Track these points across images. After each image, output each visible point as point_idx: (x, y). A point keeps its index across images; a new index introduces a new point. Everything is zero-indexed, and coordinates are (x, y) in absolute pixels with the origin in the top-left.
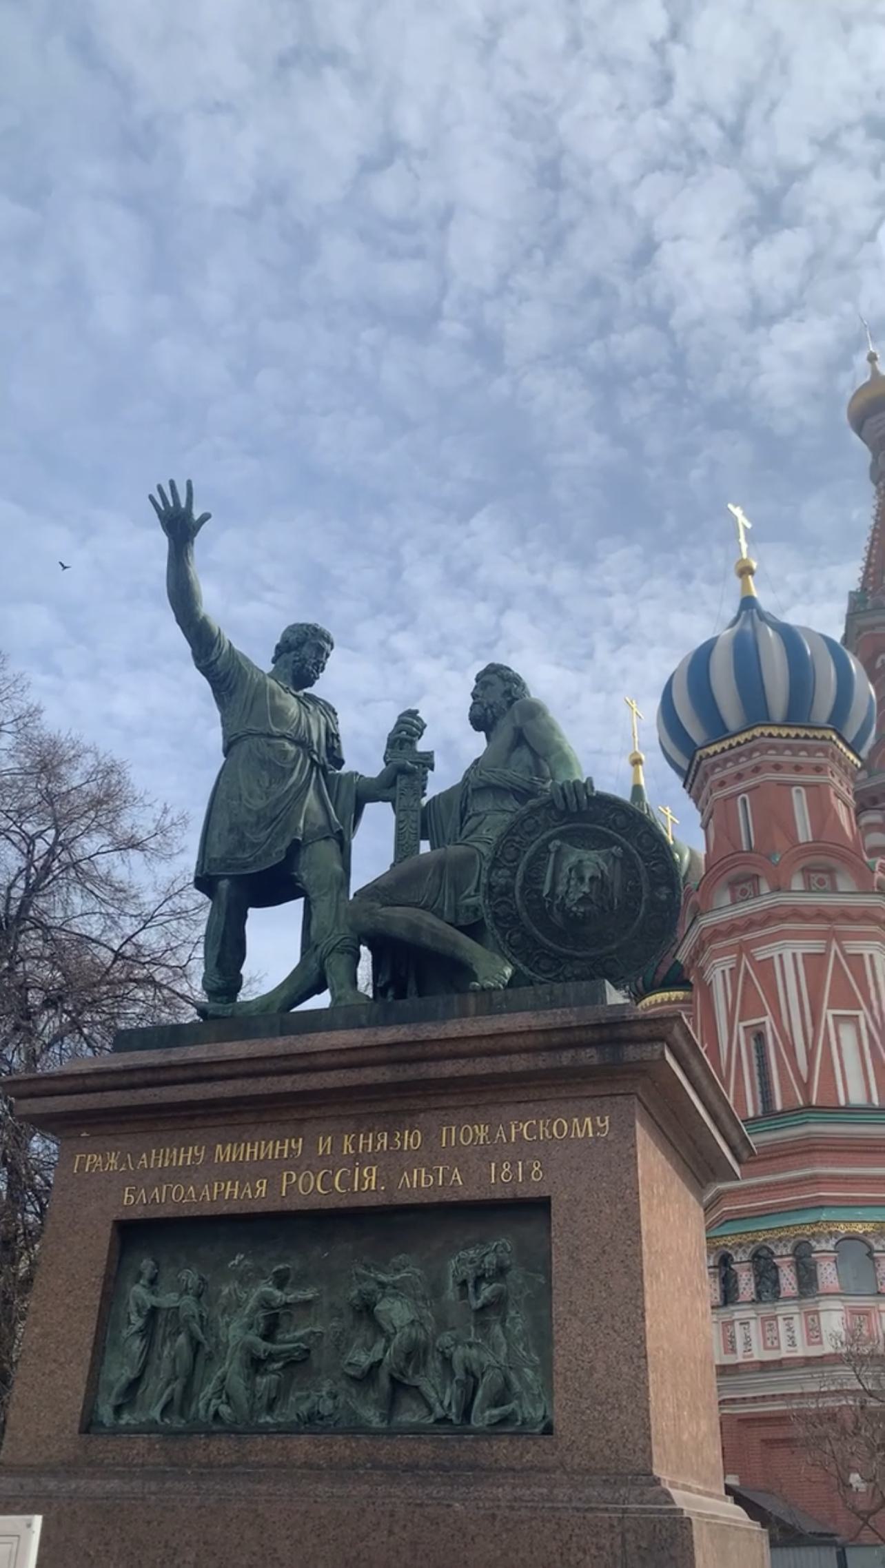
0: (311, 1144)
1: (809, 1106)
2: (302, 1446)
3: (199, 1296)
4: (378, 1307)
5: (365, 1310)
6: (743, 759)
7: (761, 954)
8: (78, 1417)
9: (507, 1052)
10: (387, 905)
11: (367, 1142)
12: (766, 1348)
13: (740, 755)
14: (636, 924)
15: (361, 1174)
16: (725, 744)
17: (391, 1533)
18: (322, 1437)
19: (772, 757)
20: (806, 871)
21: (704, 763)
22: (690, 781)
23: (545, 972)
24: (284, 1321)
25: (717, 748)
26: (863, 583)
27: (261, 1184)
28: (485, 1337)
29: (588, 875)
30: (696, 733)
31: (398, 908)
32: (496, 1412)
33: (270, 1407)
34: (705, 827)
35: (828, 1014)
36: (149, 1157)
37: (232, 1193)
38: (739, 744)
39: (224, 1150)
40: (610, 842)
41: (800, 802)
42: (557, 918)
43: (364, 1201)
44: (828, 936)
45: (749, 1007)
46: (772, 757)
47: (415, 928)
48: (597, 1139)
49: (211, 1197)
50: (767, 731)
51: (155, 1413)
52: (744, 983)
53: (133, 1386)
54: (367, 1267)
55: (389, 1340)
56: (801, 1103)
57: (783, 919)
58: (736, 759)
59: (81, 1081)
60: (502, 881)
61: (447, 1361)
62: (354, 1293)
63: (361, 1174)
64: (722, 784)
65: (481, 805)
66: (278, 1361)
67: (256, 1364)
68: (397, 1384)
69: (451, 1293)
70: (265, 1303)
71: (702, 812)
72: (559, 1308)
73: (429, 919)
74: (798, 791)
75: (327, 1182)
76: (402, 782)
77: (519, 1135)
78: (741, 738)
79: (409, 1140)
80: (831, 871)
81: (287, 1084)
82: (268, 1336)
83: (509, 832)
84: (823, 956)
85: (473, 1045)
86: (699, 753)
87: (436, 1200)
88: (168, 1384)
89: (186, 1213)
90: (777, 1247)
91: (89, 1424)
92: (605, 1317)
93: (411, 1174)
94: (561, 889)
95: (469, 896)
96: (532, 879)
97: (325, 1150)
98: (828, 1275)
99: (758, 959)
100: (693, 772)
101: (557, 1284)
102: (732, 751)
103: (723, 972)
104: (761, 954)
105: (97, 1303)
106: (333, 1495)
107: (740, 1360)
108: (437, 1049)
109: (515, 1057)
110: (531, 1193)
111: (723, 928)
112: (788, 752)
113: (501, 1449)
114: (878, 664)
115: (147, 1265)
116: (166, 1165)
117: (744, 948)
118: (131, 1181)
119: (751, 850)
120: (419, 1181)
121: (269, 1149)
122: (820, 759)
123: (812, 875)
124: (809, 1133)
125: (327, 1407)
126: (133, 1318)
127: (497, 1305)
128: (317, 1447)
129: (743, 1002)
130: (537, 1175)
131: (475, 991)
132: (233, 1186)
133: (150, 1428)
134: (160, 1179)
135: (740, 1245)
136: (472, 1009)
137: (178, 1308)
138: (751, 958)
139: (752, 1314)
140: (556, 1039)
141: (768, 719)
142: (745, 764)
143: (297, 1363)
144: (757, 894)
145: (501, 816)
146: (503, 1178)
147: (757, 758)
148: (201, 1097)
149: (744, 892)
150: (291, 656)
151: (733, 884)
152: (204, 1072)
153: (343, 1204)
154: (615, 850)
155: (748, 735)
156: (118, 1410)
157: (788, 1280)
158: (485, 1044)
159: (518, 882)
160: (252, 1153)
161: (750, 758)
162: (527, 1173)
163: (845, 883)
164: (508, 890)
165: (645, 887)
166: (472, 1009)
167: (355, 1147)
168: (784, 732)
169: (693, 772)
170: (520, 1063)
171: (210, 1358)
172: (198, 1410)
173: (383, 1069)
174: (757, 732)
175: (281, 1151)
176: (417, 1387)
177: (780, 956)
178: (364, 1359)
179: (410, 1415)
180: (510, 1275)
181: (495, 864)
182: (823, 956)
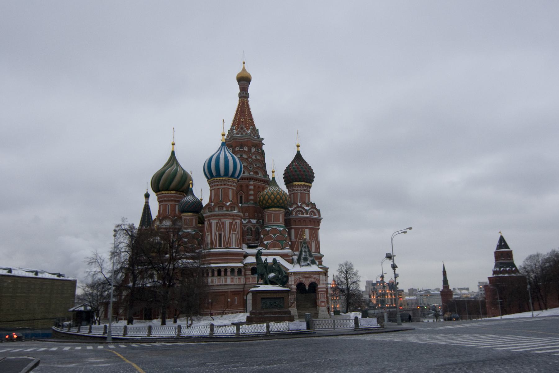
7: (223, 220)
30: (214, 173)
34: (211, 190)
44: (233, 219)
45: (220, 230)
46: (228, 183)
58: (221, 181)
64: (218, 185)
98: (229, 273)
104: (223, 220)
114: (236, 150)
117: (220, 219)
122: (235, 184)
142: (222, 183)
147: (225, 183)
151: (219, 207)
157: (223, 273)
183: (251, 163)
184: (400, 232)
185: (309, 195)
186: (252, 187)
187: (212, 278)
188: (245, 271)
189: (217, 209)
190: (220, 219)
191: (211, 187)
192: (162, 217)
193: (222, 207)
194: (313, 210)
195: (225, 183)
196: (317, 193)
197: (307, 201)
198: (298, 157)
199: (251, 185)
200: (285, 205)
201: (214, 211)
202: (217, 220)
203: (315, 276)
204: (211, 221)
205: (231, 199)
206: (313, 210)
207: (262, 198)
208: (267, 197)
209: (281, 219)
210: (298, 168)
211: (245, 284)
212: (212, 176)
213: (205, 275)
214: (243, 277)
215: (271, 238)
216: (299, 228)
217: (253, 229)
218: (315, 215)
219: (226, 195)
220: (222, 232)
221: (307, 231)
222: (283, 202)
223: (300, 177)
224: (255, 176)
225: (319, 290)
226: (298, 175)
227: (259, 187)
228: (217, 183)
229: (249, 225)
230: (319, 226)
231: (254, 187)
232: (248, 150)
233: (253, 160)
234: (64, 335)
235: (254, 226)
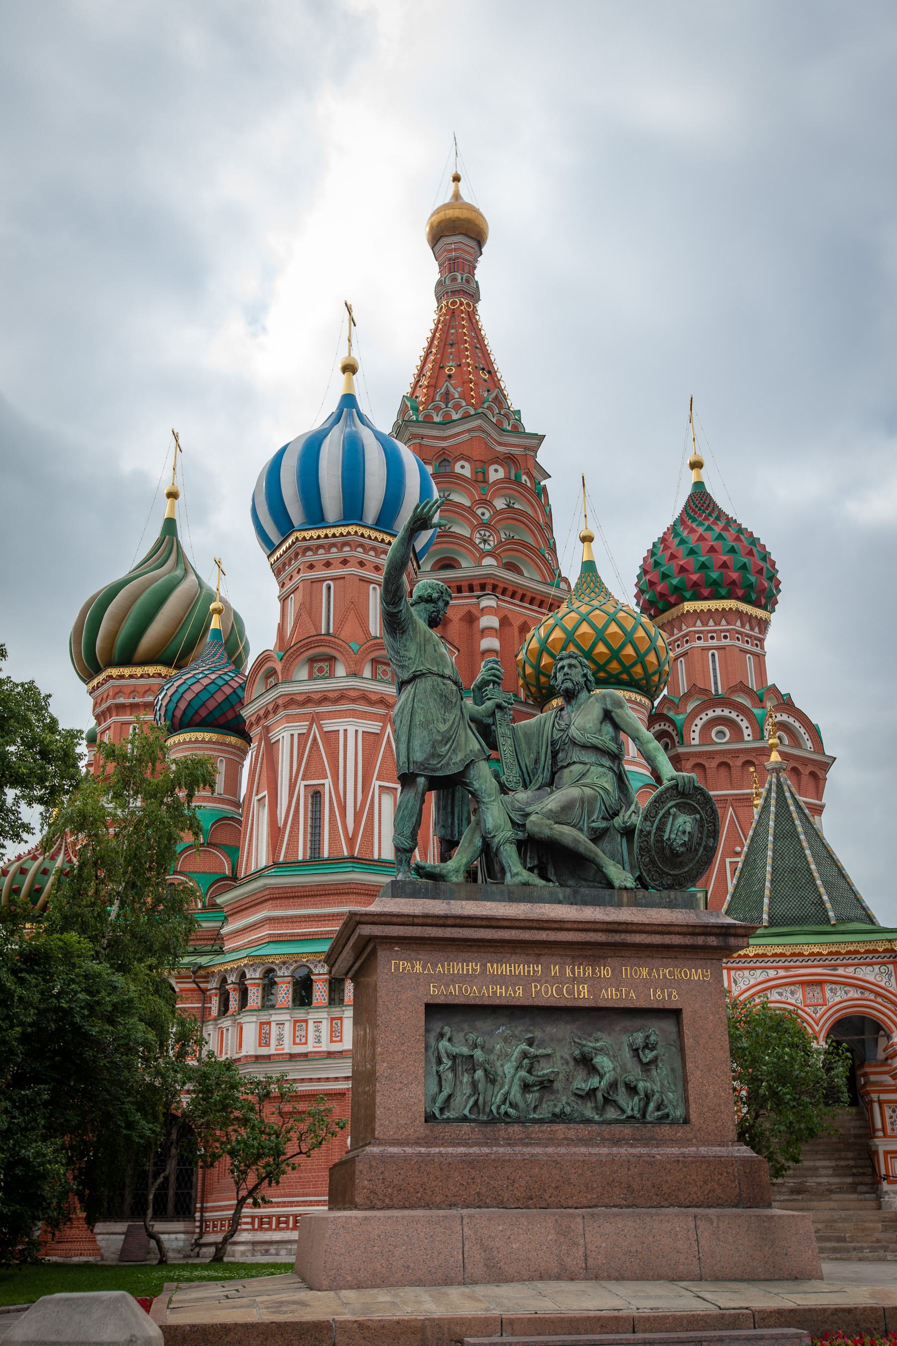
0: (547, 969)
1: (353, 857)
2: (560, 1129)
3: (483, 1048)
4: (595, 1060)
5: (585, 1062)
6: (334, 550)
7: (329, 725)
8: (423, 1115)
9: (669, 933)
10: (556, 823)
11: (579, 971)
12: (295, 1043)
13: (333, 545)
14: (697, 858)
15: (578, 988)
16: (322, 533)
17: (629, 1169)
18: (572, 1125)
19: (359, 553)
20: (375, 662)
21: (299, 544)
22: (278, 554)
23: (655, 881)
24: (536, 1065)
25: (314, 534)
26: (414, 389)
27: (519, 989)
28: (648, 1076)
29: (688, 829)
31: (565, 826)
32: (660, 1113)
33: (534, 1111)
34: (284, 599)
35: (376, 784)
36: (443, 966)
37: (501, 993)
38: (334, 536)
39: (492, 967)
40: (694, 811)
42: (668, 852)
43: (581, 1004)
45: (312, 768)
47: (575, 840)
48: (704, 981)
49: (489, 993)
50: (360, 530)
51: (466, 1112)
52: (311, 748)
53: (450, 1097)
54: (580, 1039)
55: (602, 1077)
56: (346, 854)
57: (354, 700)
59: (411, 919)
60: (648, 829)
61: (632, 1090)
62: (577, 1052)
63: (578, 988)
64: (311, 567)
65: (589, 757)
66: (536, 1086)
67: (526, 1087)
68: (607, 1100)
69: (627, 1054)
70: (525, 1055)
71: (283, 585)
72: (689, 1065)
73: (581, 835)
74: (374, 589)
75: (559, 991)
76: (498, 715)
77: (664, 975)
78: (337, 531)
79: (605, 972)
81: (543, 936)
82: (529, 1072)
83: (655, 801)
84: (378, 736)
85: (654, 928)
86: (298, 534)
87: (622, 1006)
88: (469, 1097)
89: (473, 1002)
90: (316, 966)
91: (430, 1118)
92: (713, 1069)
93: (607, 991)
94: (673, 836)
95: (593, 821)
96: (661, 829)
97: (556, 973)
99: (325, 729)
100: (284, 548)
101: (687, 1052)
102: (326, 541)
103: (292, 735)
105: (423, 1050)
106: (590, 1154)
107: (273, 1052)
108: (634, 928)
109: (672, 937)
110: (673, 1006)
111: (299, 698)
112: (372, 553)
113: (665, 1130)
115: (447, 1029)
116: (456, 972)
117: (315, 719)
118: (433, 980)
119: (328, 634)
120: (612, 995)
121: (521, 969)
123: (380, 666)
124: (352, 879)
125: (568, 1110)
126: (445, 1060)
127: (654, 1061)
128: (569, 1129)
129: (307, 764)
130: (675, 997)
131: (620, 889)
132: (501, 988)
133: (465, 1119)
134: (453, 980)
135: (284, 963)
136: (625, 900)
137: (472, 1056)
138: (320, 728)
139: (287, 1017)
140: (697, 930)
141: (361, 520)
143: (546, 1085)
144: (331, 675)
145: (600, 769)
146: (657, 997)
148: (490, 937)
149: (321, 670)
150: (430, 607)
151: (312, 660)
152: (494, 923)
153: (569, 1004)
154: (698, 816)
155: (344, 530)
156: (442, 1110)
158: (660, 928)
159: (654, 831)
160: (511, 971)
161: (340, 550)
162: (670, 995)
164: (649, 833)
165: (705, 839)
166: (625, 900)
167: (573, 971)
168: (374, 534)
169: (284, 548)
170: (676, 940)
171: (493, 1082)
172: (491, 1110)
173: (600, 934)
174: (352, 529)
175: (529, 972)
176: (614, 1101)
177: (346, 731)
178: (586, 1087)
179: (612, 1114)
180: (659, 1046)
181: (646, 818)
182: (378, 736)
183: (486, 526)
185: (760, 658)
187: (264, 1017)
193: (332, 659)
194: (784, 718)
197: (752, 683)
198: (700, 503)
200: (647, 676)
201: (287, 681)
202: (301, 727)
204: (274, 736)
206: (784, 718)
207: (534, 644)
210: (701, 538)
212: (285, 526)
213: (233, 1004)
222: (640, 659)
223: (714, 575)
226: (703, 566)
230: (819, 795)
231: (505, 621)
232: (475, 472)
233: (497, 513)
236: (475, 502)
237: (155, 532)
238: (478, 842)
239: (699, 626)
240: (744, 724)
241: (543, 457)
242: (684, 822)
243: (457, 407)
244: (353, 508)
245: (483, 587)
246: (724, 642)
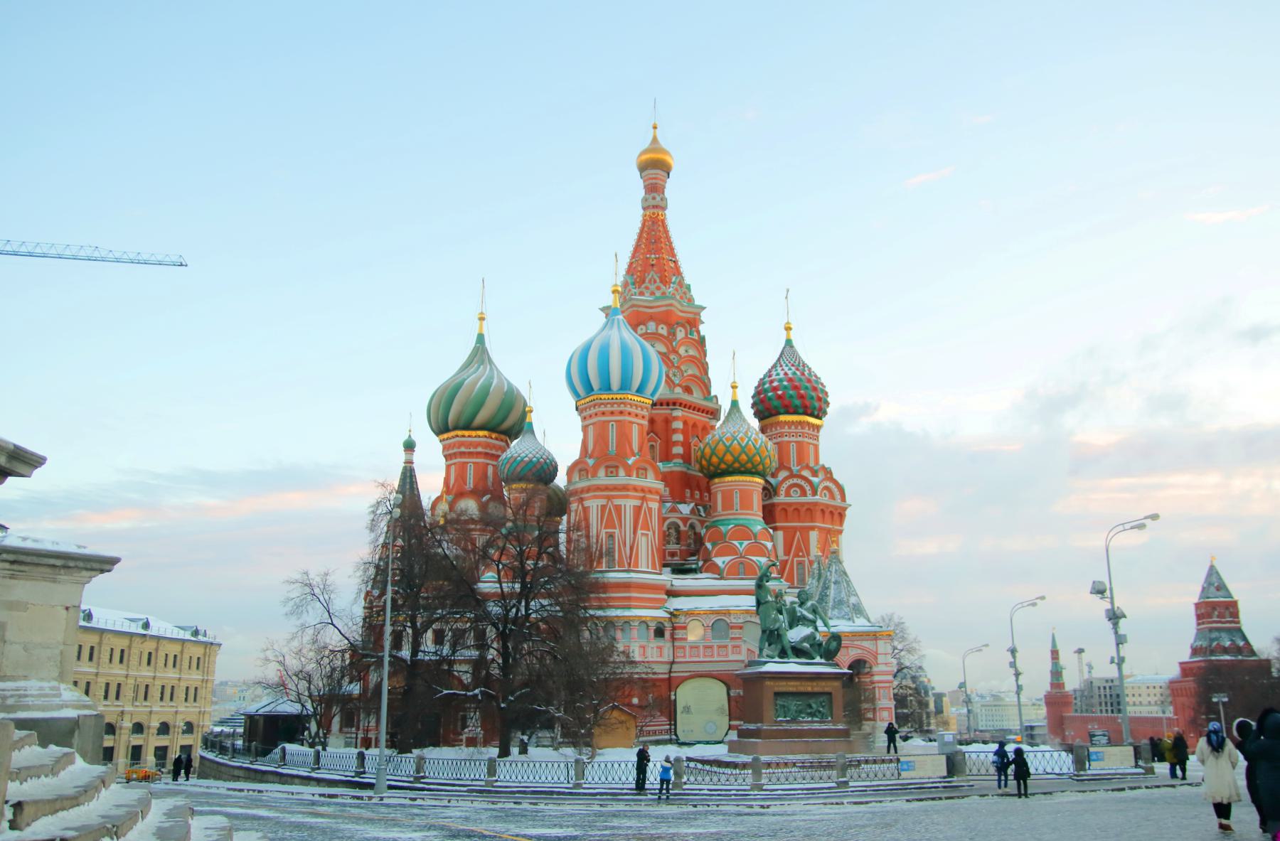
5: (810, 707)
7: (617, 502)
20: (638, 469)
30: (595, 385)
34: (585, 429)
35: (639, 532)
41: (635, 429)
44: (643, 499)
46: (628, 409)
64: (603, 413)
80: (645, 469)
104: (617, 502)
117: (609, 498)
122: (645, 413)
146: (827, 690)
151: (607, 467)
163: (650, 474)
184: (1127, 526)
185: (816, 447)
186: (678, 425)
188: (674, 628)
189: (602, 472)
190: (609, 498)
191: (584, 419)
192: (454, 491)
193: (617, 467)
195: (622, 408)
196: (837, 443)
197: (812, 464)
199: (676, 418)
202: (603, 502)
203: (866, 644)
204: (586, 503)
205: (636, 450)
208: (721, 446)
209: (757, 501)
211: (673, 663)
212: (589, 388)
214: (669, 645)
215: (732, 551)
216: (795, 529)
217: (682, 528)
218: (832, 497)
219: (624, 437)
220: (617, 531)
221: (814, 536)
224: (686, 397)
225: (876, 678)
227: (694, 425)
228: (602, 409)
229: (673, 518)
230: (841, 523)
231: (685, 423)
232: (669, 334)
234: (236, 773)
235: (685, 520)
236: (669, 352)
237: (471, 344)
238: (779, 647)
239: (786, 429)
240: (808, 488)
241: (703, 316)
242: (834, 644)
243: (658, 288)
244: (625, 386)
245: (674, 404)
246: (800, 439)
